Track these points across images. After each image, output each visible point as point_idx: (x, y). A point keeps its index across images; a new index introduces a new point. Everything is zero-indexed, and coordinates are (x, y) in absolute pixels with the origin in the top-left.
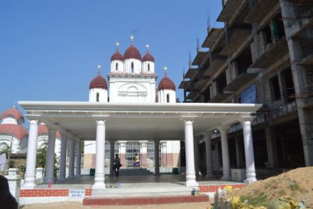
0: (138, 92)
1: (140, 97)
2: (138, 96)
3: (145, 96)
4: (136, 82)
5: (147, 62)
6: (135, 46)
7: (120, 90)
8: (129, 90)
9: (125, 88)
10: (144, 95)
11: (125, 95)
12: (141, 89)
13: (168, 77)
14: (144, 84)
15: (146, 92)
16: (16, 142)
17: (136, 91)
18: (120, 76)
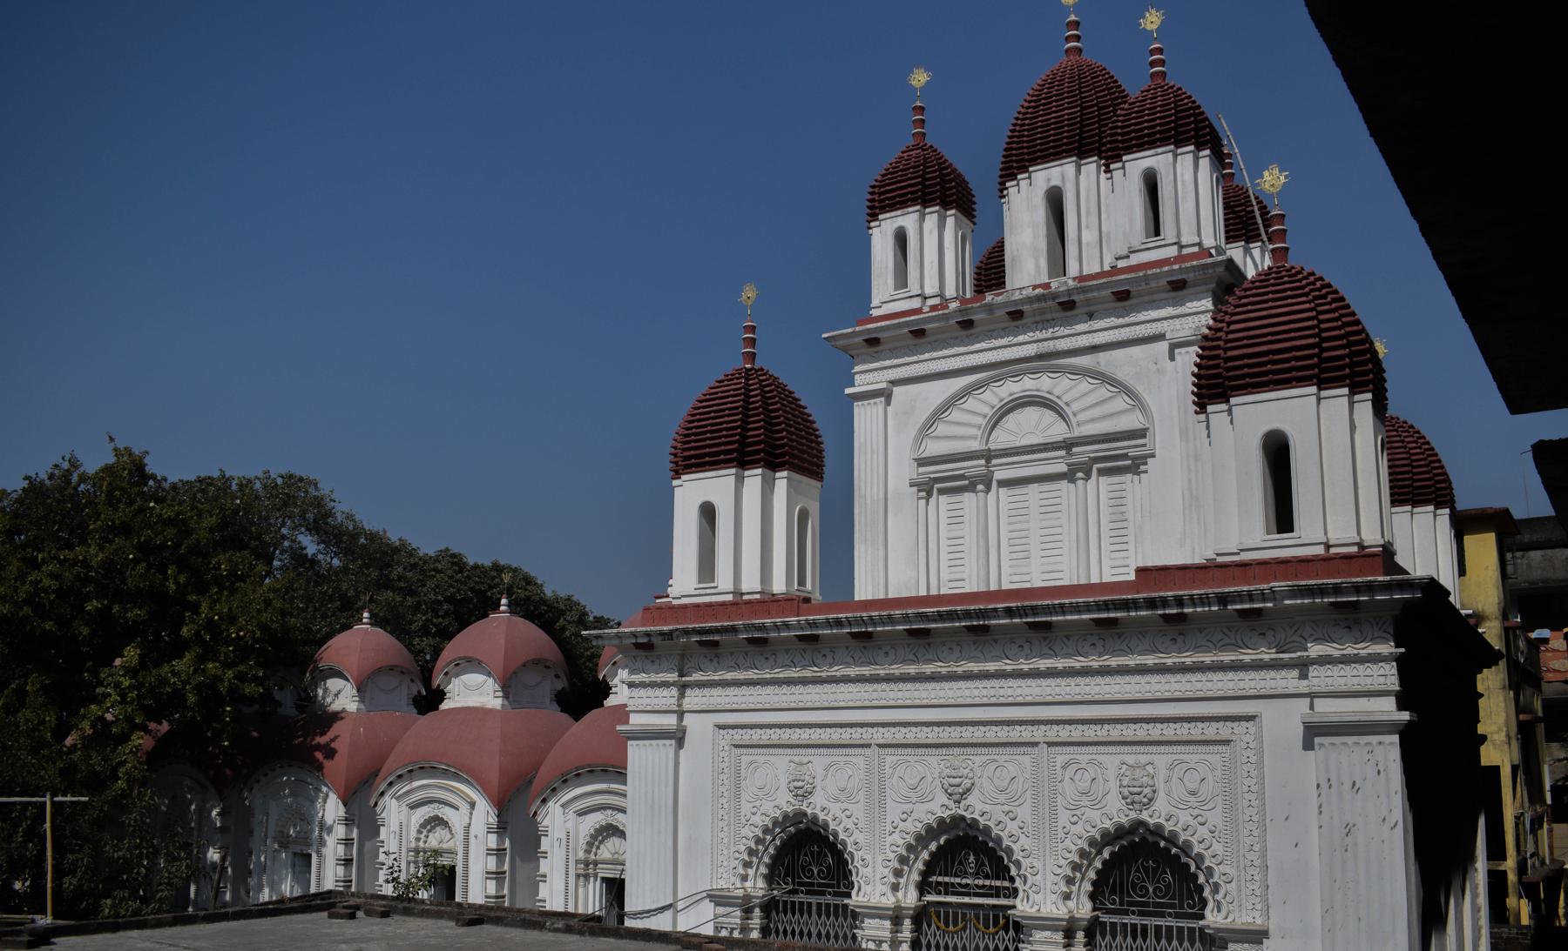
0: (1068, 445)
1: (1101, 487)
2: (1069, 476)
3: (1136, 466)
4: (1045, 361)
5: (1137, 164)
6: (1093, 56)
7: (933, 448)
8: (1001, 439)
9: (963, 432)
10: (1121, 456)
11: (971, 485)
12: (1092, 410)
13: (1293, 261)
14: (1103, 360)
15: (1141, 433)
16: (485, 814)
17: (1059, 431)
18: (919, 333)
